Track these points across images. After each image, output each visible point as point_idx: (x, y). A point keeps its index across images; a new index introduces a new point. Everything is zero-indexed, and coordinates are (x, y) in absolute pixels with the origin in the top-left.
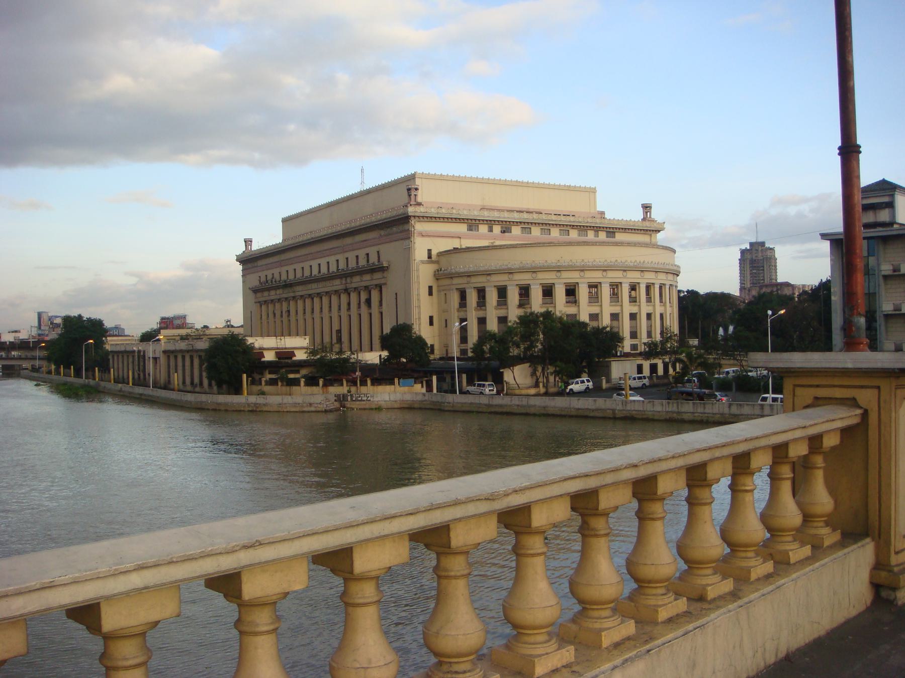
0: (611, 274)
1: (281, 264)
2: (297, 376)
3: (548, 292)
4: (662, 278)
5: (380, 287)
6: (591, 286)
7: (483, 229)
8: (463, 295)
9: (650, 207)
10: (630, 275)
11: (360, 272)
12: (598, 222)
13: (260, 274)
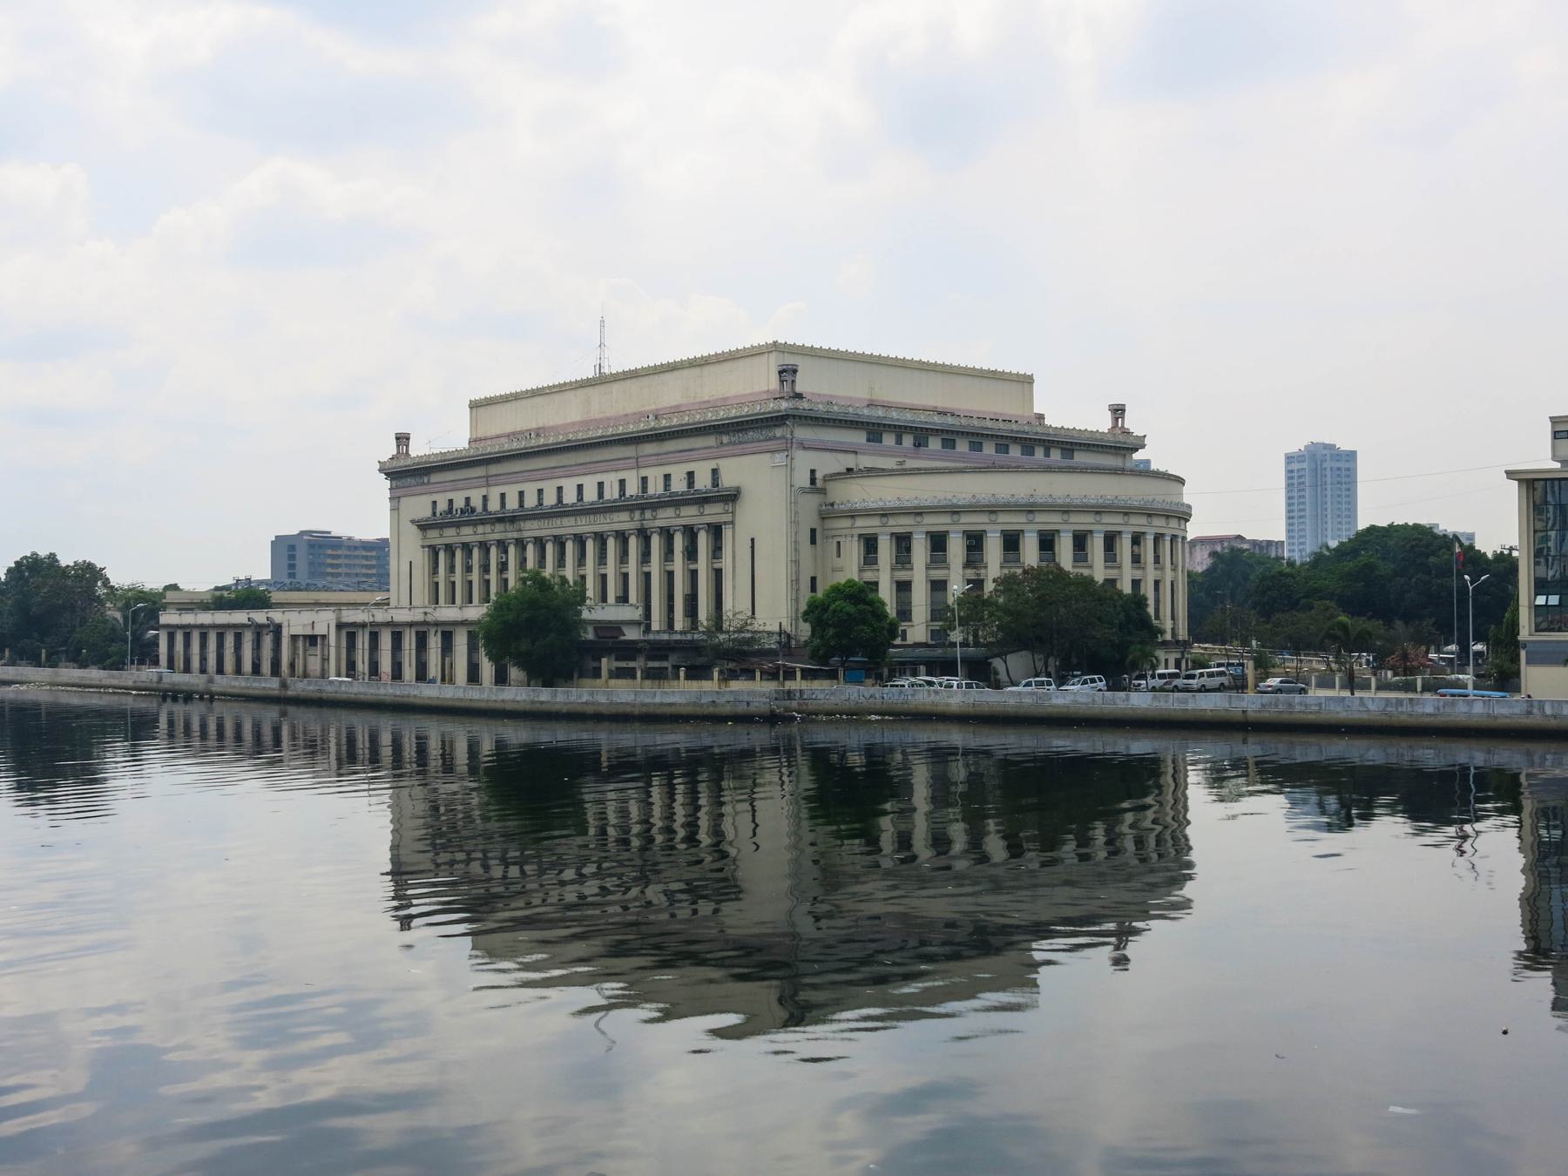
0: (1106, 519)
1: (488, 481)
2: (665, 664)
3: (1047, 543)
4: (1151, 528)
5: (716, 531)
7: (889, 440)
8: (870, 544)
9: (1123, 411)
10: (1134, 520)
11: (676, 502)
12: (1032, 431)
13: (435, 497)
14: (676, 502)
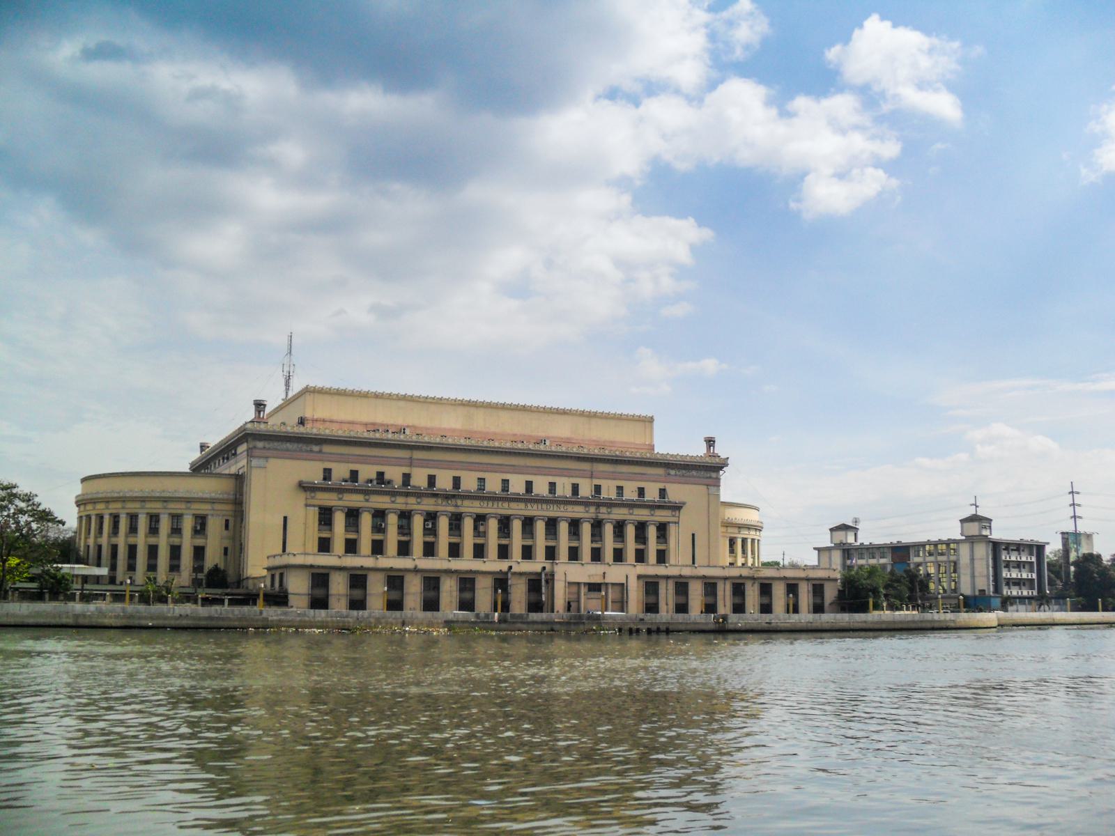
1: (411, 463)
6: (197, 517)
11: (631, 505)
14: (631, 505)
